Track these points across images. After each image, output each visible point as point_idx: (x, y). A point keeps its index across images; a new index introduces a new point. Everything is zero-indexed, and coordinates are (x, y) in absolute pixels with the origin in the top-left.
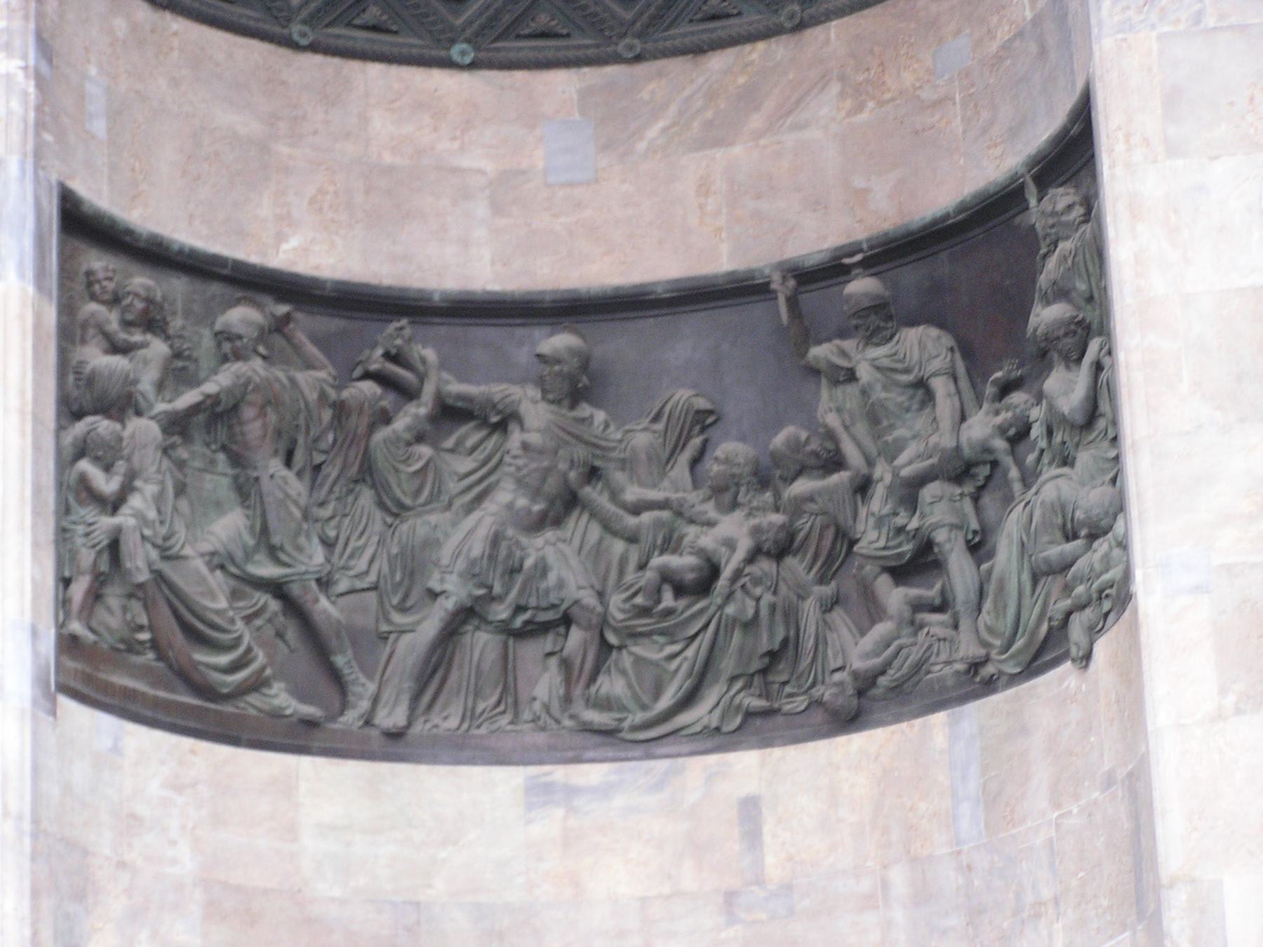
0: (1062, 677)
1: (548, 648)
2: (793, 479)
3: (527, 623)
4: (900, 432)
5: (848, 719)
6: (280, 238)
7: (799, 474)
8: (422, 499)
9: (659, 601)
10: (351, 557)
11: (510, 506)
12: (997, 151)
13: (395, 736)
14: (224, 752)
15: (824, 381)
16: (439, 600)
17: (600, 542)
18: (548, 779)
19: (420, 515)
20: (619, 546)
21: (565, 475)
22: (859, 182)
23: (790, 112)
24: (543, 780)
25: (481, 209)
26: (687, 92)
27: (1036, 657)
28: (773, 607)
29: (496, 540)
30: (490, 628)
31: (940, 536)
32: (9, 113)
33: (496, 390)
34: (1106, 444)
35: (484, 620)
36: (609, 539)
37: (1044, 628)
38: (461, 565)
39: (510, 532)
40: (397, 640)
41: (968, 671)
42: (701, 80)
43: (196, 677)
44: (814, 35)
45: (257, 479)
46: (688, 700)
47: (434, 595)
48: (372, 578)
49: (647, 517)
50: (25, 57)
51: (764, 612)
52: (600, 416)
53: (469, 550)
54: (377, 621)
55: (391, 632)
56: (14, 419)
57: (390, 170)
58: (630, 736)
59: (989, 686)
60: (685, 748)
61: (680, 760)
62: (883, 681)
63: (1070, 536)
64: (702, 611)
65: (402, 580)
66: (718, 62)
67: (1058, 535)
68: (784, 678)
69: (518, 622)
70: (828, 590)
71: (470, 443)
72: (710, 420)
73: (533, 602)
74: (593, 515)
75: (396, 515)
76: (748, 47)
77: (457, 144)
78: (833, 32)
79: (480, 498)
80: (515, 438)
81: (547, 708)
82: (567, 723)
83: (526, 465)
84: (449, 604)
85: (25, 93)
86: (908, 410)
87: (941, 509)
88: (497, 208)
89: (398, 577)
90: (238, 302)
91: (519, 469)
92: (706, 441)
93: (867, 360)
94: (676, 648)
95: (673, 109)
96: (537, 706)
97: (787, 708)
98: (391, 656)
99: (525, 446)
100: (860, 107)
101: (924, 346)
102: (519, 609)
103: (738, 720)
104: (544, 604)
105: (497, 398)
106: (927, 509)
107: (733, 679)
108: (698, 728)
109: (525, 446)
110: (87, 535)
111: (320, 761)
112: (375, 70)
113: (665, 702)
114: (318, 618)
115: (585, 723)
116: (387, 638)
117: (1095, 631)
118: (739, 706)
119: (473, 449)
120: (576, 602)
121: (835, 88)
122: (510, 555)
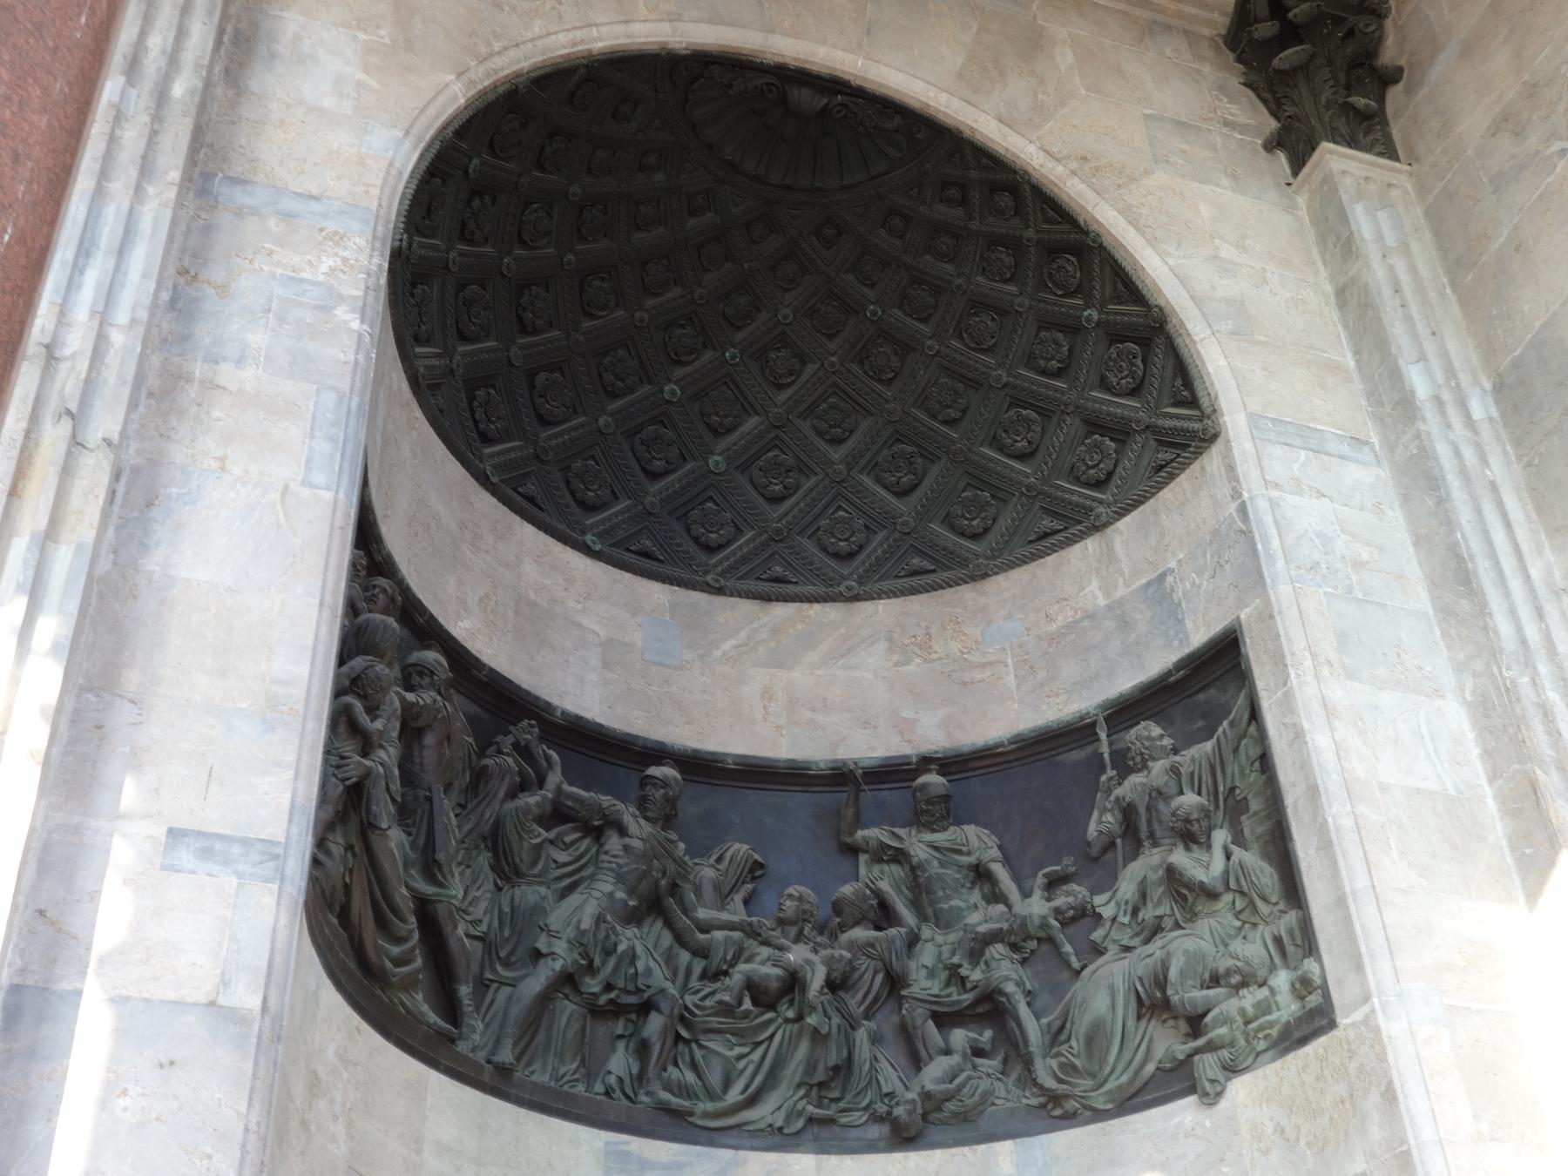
0: (1183, 1112)
1: (619, 1031)
2: (853, 926)
3: (612, 1001)
4: (956, 902)
5: (904, 1137)
6: (459, 617)
7: (857, 923)
8: (536, 871)
9: (740, 1004)
10: (471, 904)
11: (611, 895)
12: (1062, 698)
13: (504, 1071)
14: (378, 1039)
15: (863, 858)
16: (542, 961)
17: (670, 948)
18: (625, 1148)
19: (530, 884)
20: (684, 957)
21: (657, 882)
22: (907, 713)
23: (842, 656)
24: (621, 1147)
25: (595, 661)
26: (755, 625)
27: (1130, 1098)
28: (839, 1026)
29: (599, 919)
30: (577, 999)
31: (1010, 988)
32: (356, 363)
33: (606, 800)
34: (1230, 916)
35: (577, 990)
36: (677, 948)
37: (1150, 1068)
38: (570, 932)
39: (609, 918)
40: (497, 990)
41: (1043, 1106)
42: (766, 620)
43: (372, 955)
44: (866, 607)
45: (429, 799)
46: (752, 1101)
47: (537, 955)
48: (484, 928)
49: (718, 935)
50: (371, 327)
51: (835, 1030)
52: (682, 846)
53: (579, 921)
54: (482, 967)
55: (493, 981)
56: (326, 614)
57: (534, 604)
58: (700, 1122)
59: (1069, 1119)
60: (747, 1142)
61: (741, 1153)
62: (951, 1106)
63: (1215, 980)
64: (770, 1021)
65: (511, 935)
66: (780, 611)
67: (1199, 982)
68: (835, 1094)
69: (603, 1000)
70: (872, 1025)
71: (568, 839)
72: (759, 873)
73: (621, 984)
74: (668, 924)
75: (508, 880)
76: (805, 606)
77: (580, 606)
78: (881, 608)
79: (572, 888)
80: (614, 842)
81: (620, 1080)
82: (644, 1098)
83: (626, 864)
84: (558, 965)
85: (368, 353)
86: (963, 886)
87: (1004, 969)
88: (606, 664)
89: (507, 933)
90: (428, 647)
91: (619, 866)
92: (754, 890)
93: (919, 845)
94: (746, 1050)
95: (743, 634)
96: (612, 1080)
97: (843, 1120)
98: (493, 1001)
99: (626, 848)
100: (908, 662)
101: (978, 841)
102: (609, 987)
103: (800, 1124)
104: (631, 987)
105: (605, 805)
106: (993, 964)
107: (799, 1085)
108: (763, 1126)
109: (626, 848)
110: (338, 767)
111: (444, 1079)
112: (529, 529)
113: (734, 1095)
114: (453, 944)
115: (661, 1102)
116: (488, 987)
117: (1232, 1070)
118: (800, 1113)
119: (573, 843)
120: (663, 990)
121: (882, 646)
122: (607, 936)
